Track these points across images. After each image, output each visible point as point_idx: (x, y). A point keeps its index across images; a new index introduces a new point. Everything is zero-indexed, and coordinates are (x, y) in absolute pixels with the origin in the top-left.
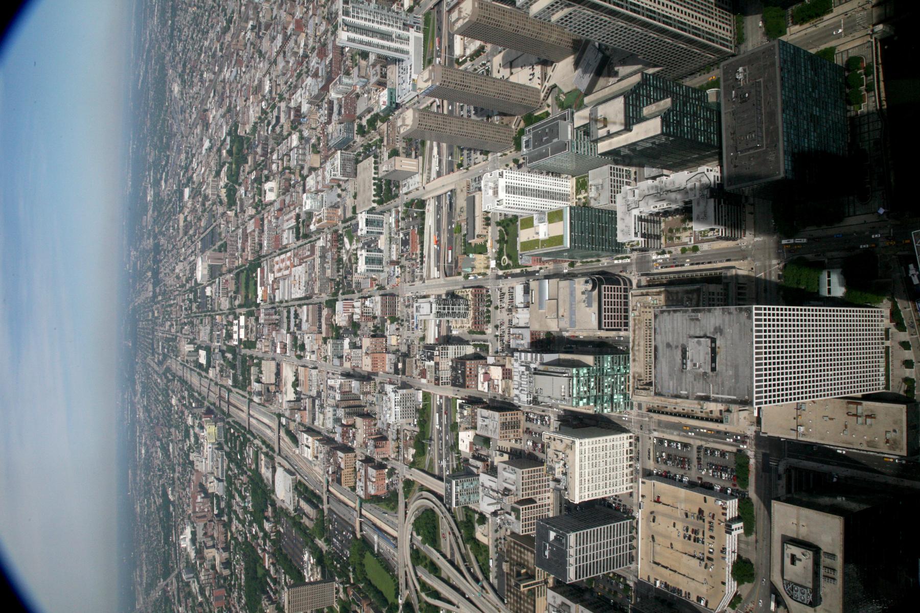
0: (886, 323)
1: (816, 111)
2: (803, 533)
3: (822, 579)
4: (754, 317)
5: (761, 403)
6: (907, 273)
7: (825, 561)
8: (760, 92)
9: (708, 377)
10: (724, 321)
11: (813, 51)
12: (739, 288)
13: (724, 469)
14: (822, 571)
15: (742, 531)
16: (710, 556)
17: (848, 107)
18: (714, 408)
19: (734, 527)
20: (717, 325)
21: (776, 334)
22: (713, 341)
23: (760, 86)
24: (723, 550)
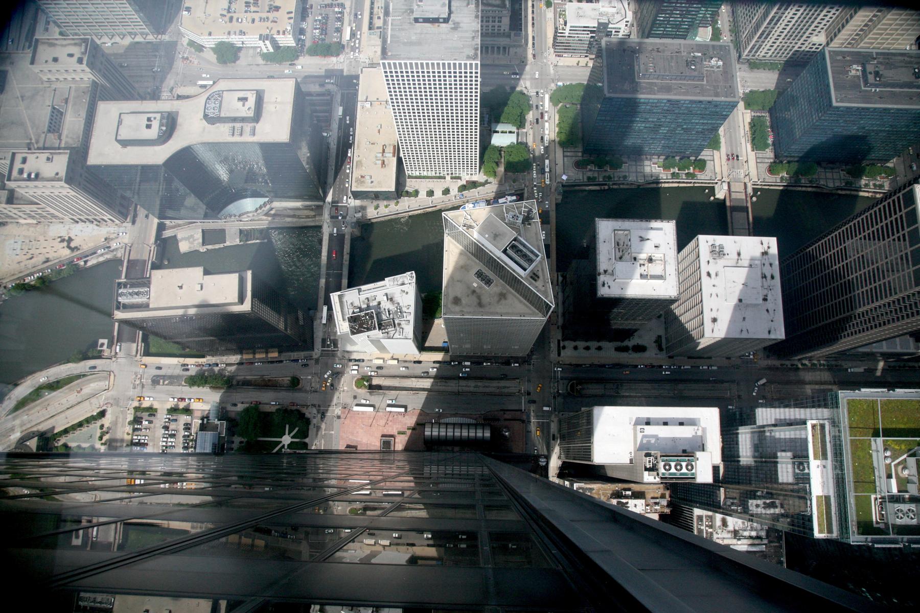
0: (466, 178)
1: (663, 130)
2: (268, 108)
3: (231, 125)
4: (468, 62)
5: (385, 68)
6: (509, 195)
7: (248, 127)
8: (693, 80)
9: (409, 14)
10: (466, 31)
11: (721, 131)
12: (504, 48)
13: (324, 31)
14: (238, 125)
15: (265, 51)
16: (234, 20)
17: (663, 157)
18: (378, 23)
19: (267, 42)
20: (461, 25)
21: (453, 83)
22: (446, 20)
23: (699, 80)
24: (242, 33)
